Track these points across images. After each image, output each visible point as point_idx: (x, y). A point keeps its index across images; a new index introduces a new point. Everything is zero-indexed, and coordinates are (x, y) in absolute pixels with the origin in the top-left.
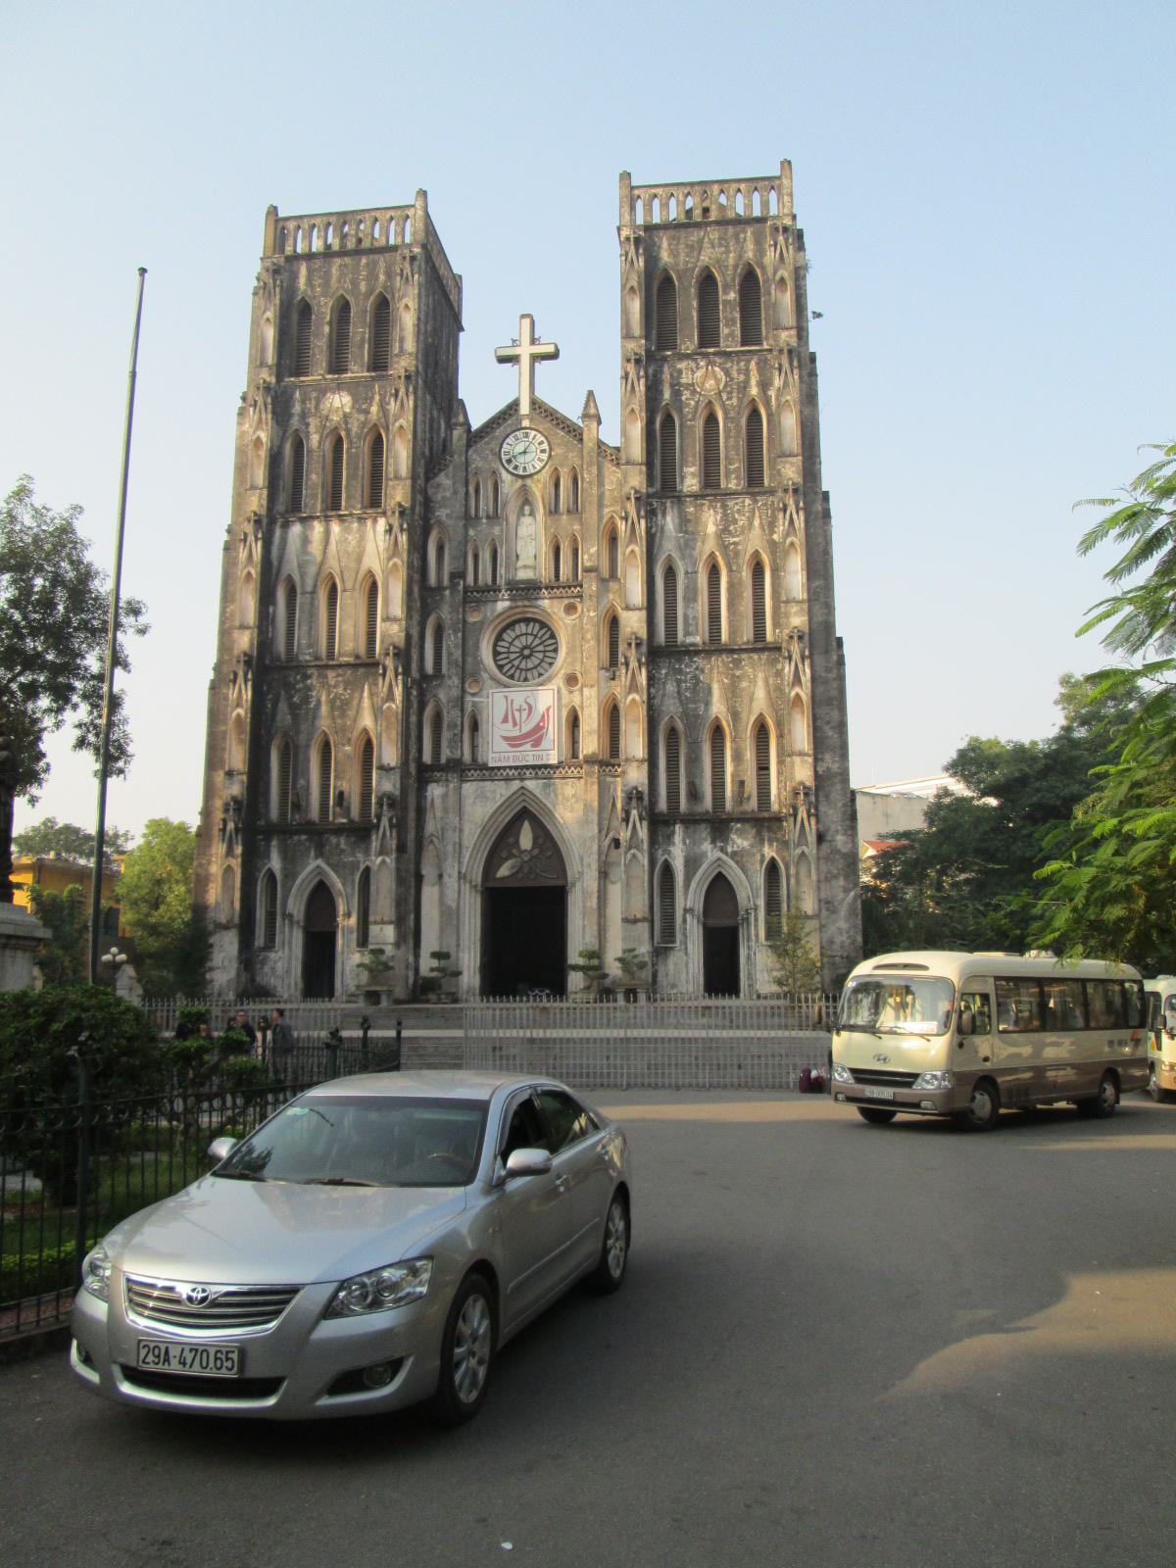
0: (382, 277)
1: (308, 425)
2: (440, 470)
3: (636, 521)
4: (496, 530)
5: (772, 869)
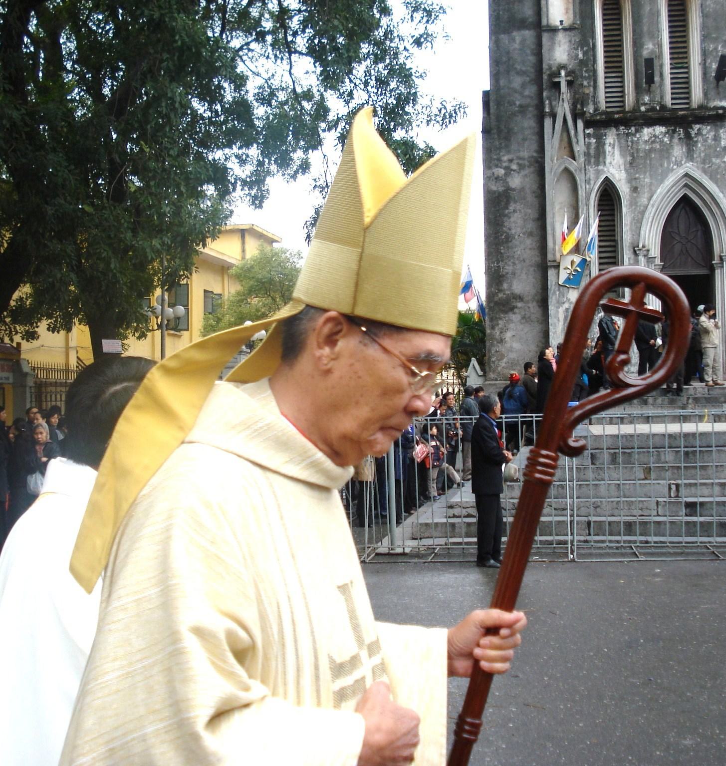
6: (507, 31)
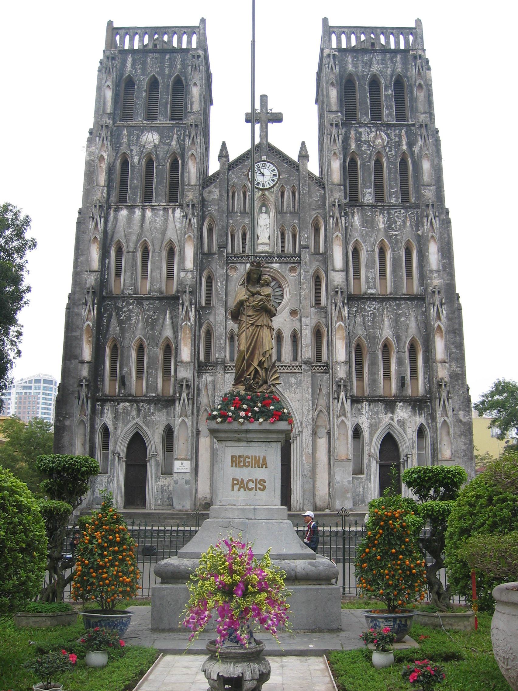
1: (131, 150)
2: (211, 183)
3: (339, 218)
4: (247, 221)
5: (421, 433)
6: (69, 360)
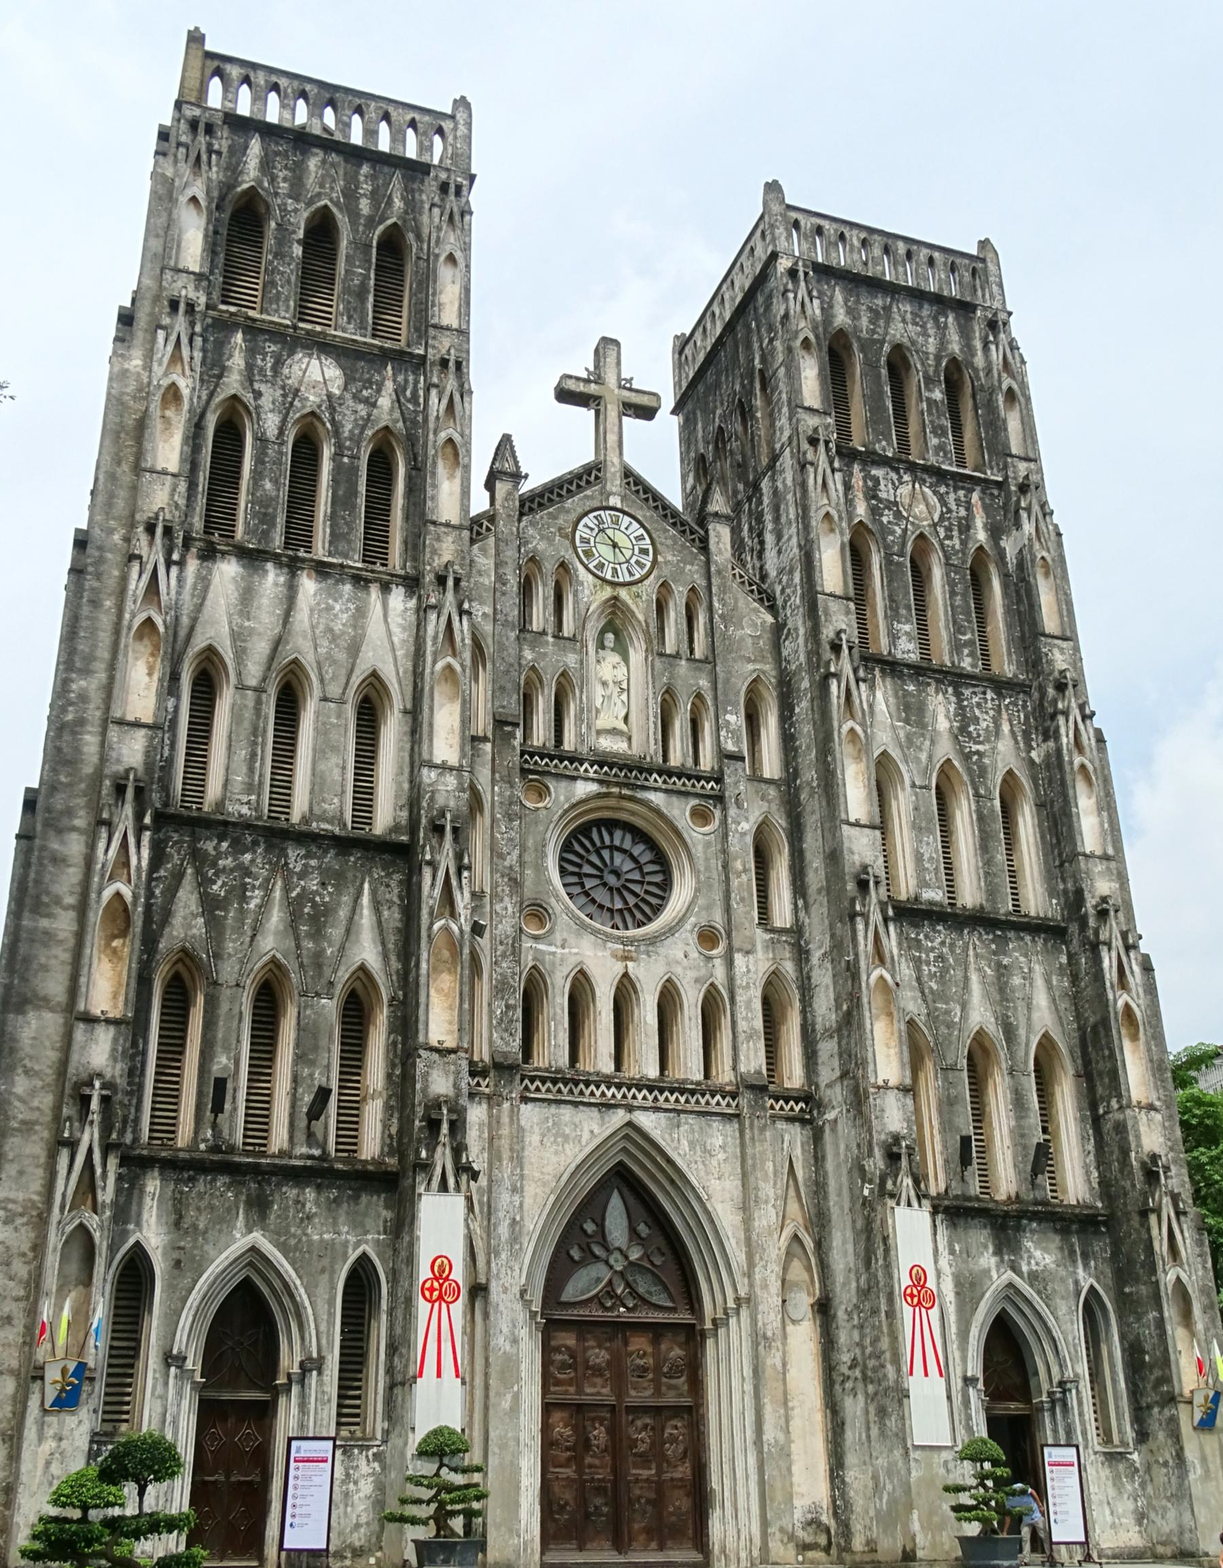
0: (398, 203)
1: (258, 395)
4: (571, 659)
